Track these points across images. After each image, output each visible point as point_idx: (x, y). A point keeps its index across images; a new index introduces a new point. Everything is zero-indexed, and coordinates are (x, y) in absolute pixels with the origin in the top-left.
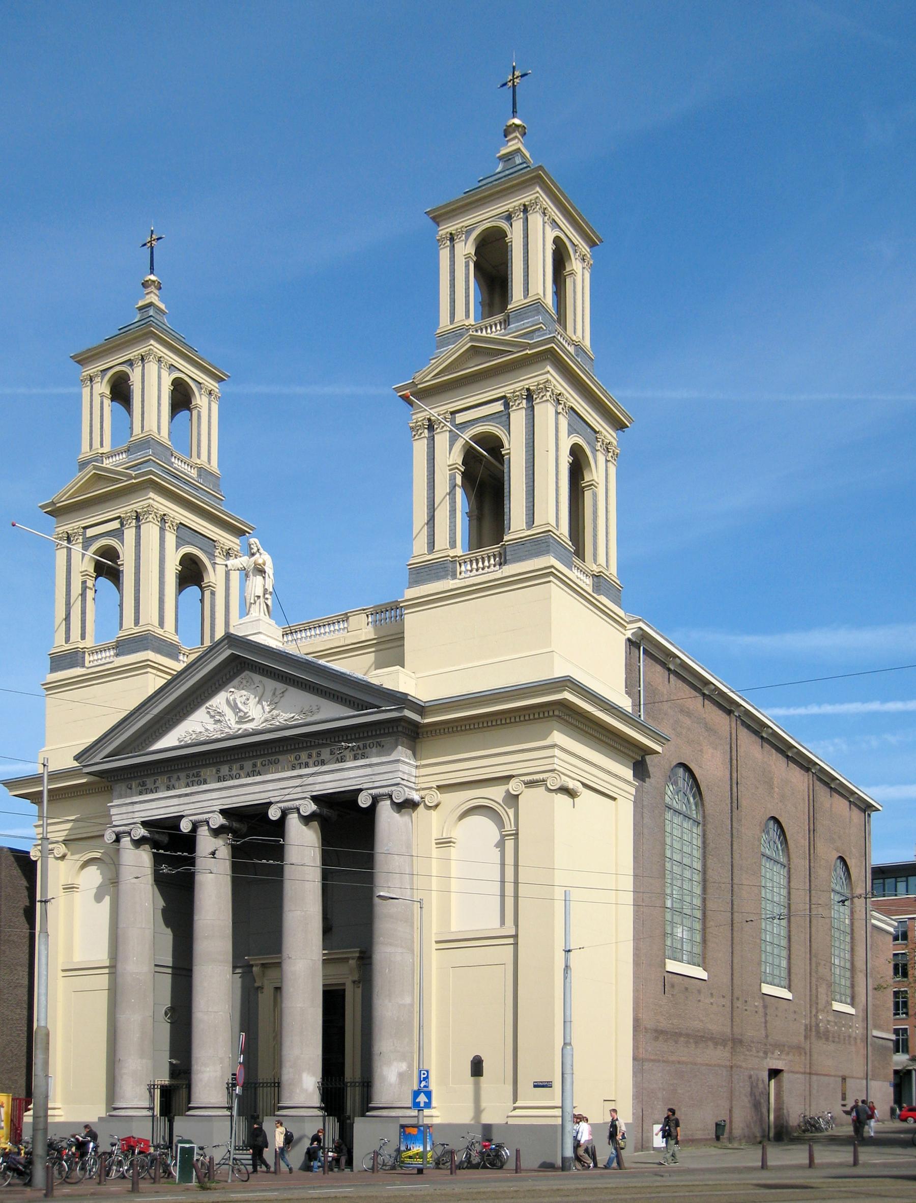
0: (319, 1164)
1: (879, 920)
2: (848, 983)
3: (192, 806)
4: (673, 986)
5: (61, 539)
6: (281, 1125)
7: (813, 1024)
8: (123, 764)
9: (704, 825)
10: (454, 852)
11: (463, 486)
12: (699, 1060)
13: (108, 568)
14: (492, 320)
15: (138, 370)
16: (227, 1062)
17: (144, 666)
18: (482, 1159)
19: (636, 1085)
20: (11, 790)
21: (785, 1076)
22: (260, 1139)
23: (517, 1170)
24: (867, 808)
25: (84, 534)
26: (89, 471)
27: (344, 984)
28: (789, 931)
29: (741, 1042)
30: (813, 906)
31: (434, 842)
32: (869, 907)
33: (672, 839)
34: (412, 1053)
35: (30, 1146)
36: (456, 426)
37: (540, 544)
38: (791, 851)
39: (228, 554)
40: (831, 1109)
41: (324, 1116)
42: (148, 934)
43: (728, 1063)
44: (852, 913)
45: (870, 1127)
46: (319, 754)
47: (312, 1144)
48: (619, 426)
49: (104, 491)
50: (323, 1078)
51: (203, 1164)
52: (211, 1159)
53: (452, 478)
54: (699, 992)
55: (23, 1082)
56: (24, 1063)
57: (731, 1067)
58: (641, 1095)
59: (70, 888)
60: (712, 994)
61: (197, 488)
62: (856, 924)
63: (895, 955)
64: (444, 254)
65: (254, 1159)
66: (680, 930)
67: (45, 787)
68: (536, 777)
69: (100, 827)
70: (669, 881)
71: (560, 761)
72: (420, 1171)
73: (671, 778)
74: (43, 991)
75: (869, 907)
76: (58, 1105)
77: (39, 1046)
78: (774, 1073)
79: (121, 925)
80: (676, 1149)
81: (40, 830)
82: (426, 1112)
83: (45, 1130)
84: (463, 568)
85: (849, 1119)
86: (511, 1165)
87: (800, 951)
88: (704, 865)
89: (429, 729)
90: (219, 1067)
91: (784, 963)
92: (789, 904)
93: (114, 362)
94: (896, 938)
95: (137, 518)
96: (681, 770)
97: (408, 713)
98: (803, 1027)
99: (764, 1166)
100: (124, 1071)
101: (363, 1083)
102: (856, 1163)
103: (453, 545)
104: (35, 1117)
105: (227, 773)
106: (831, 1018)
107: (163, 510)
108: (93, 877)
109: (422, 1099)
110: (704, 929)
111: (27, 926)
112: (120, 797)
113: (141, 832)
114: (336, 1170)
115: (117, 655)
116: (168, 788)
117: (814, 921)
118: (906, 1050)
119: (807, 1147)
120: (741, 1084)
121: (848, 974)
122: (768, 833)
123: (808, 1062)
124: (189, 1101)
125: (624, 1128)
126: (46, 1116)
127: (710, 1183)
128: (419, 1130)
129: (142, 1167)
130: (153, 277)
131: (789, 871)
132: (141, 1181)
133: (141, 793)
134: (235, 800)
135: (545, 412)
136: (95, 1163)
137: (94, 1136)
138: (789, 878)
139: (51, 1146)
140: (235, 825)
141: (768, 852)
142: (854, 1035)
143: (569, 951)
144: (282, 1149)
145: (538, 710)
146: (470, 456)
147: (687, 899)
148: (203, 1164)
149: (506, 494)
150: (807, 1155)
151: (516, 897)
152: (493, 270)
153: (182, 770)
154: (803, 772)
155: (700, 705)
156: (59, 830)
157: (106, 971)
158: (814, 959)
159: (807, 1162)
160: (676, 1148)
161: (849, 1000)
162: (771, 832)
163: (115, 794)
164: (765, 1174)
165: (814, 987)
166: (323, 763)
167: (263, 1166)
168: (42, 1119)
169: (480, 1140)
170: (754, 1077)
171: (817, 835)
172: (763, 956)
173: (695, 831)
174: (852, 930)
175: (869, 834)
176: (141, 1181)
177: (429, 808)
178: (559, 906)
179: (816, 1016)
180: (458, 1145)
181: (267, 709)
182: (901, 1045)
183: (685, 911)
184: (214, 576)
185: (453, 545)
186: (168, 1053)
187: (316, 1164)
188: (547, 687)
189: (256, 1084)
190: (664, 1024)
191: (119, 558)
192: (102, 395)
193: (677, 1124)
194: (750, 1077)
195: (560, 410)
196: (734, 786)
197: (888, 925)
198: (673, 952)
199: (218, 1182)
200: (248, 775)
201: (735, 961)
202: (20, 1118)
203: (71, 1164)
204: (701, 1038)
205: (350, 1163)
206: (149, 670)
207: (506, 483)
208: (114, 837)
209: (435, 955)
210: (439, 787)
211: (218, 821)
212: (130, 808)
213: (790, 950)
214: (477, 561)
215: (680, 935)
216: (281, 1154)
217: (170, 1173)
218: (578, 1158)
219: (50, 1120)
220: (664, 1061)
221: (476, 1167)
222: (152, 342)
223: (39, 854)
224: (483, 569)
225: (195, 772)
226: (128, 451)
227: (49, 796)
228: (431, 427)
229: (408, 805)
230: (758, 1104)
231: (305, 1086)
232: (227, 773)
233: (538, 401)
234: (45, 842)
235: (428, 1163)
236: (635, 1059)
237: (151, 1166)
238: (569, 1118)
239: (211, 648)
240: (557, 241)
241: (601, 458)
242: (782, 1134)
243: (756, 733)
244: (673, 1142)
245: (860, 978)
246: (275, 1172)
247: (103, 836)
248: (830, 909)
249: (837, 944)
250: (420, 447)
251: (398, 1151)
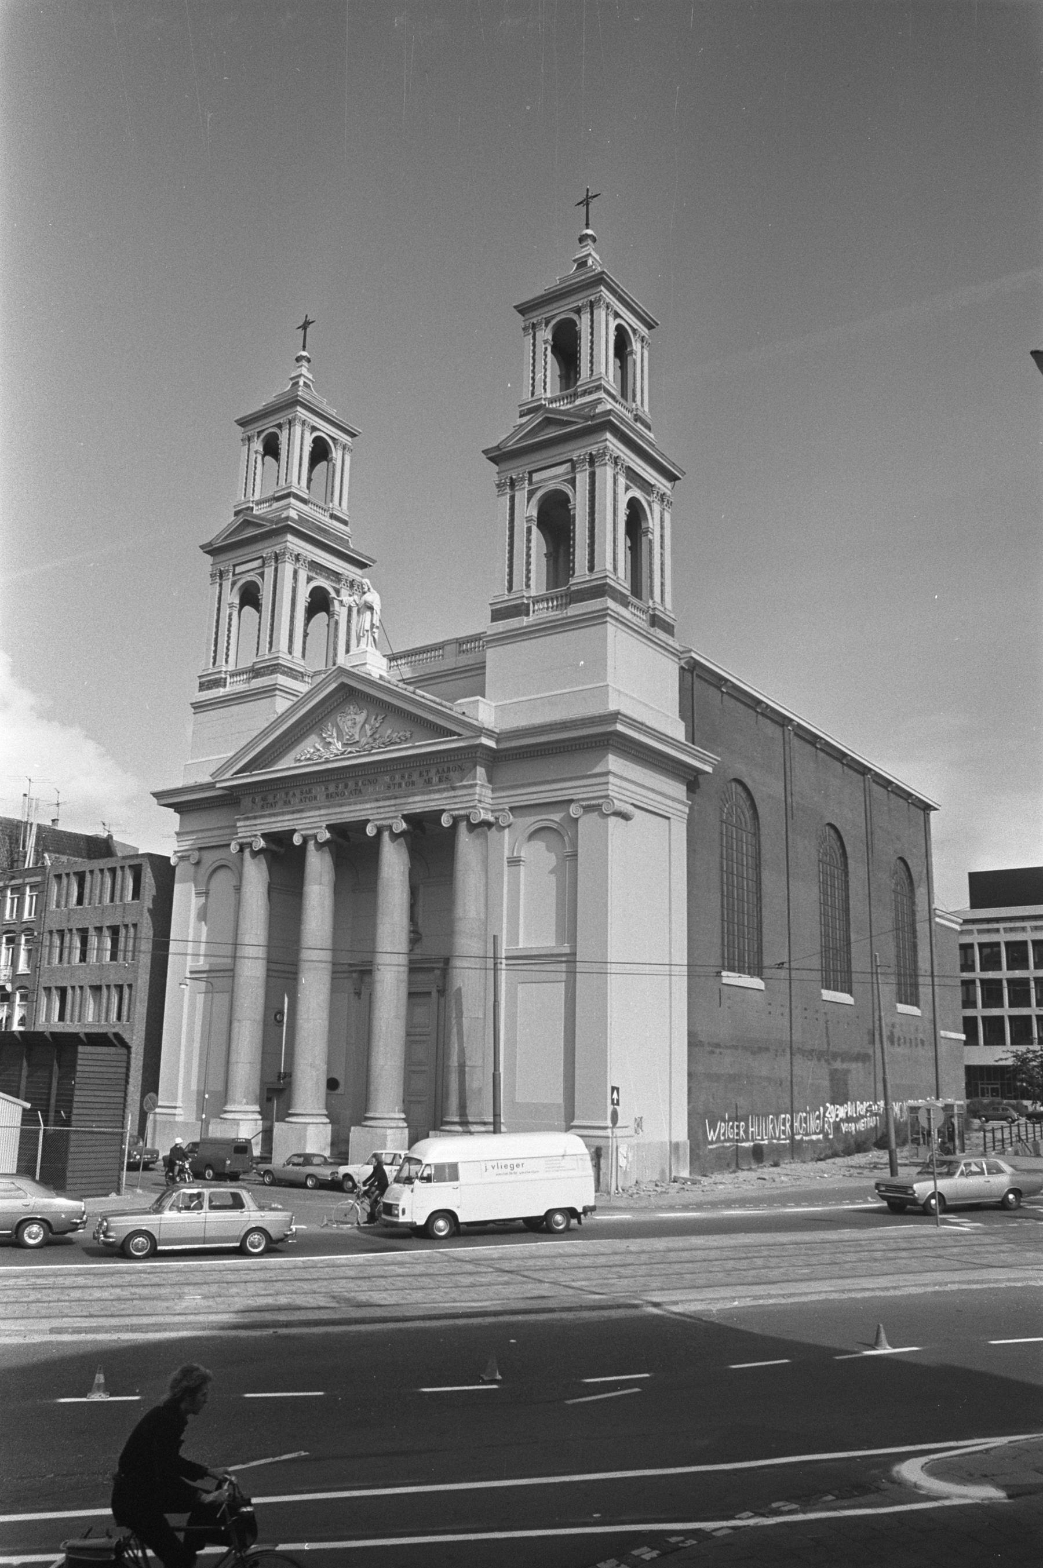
46: (410, 776)
113: (262, 843)
210: (511, 809)
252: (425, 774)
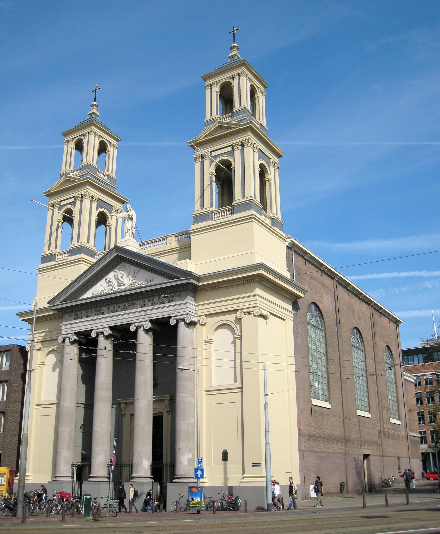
0: (150, 508)
1: (407, 376)
2: (396, 409)
3: (97, 325)
4: (315, 412)
5: (50, 206)
6: (133, 487)
7: (382, 430)
8: (69, 306)
9: (325, 332)
10: (213, 346)
11: (215, 181)
12: (330, 451)
13: (68, 218)
14: (226, 116)
15: (86, 138)
16: (108, 453)
17: (80, 260)
18: (229, 505)
19: (301, 464)
20: (20, 317)
21: (371, 458)
22: (122, 494)
23: (246, 511)
24: (396, 322)
25: (60, 204)
26: (64, 178)
27: (162, 413)
28: (367, 383)
29: (349, 440)
30: (377, 370)
31: (204, 341)
32: (403, 370)
33: (311, 339)
34: (194, 448)
35: (16, 495)
36: (212, 157)
37: (248, 205)
38: (365, 343)
39: (117, 211)
40: (393, 475)
41: (153, 482)
42: (75, 387)
43: (344, 452)
44: (395, 373)
45: (413, 483)
46: (153, 300)
47: (147, 497)
48: (279, 156)
49: (70, 186)
50: (152, 462)
51: (95, 507)
52: (99, 504)
53: (211, 178)
54: (328, 415)
55: (15, 462)
56: (16, 452)
57: (345, 454)
58: (304, 470)
59: (42, 364)
60: (334, 416)
61: (106, 184)
62: (397, 379)
63: (416, 393)
64: (208, 91)
65: (119, 505)
66: (317, 384)
67: (35, 316)
68: (249, 310)
69: (57, 335)
70: (311, 359)
71: (260, 302)
72: (199, 512)
73: (309, 309)
74: (27, 415)
75: (403, 370)
76: (30, 474)
77: (23, 443)
78: (366, 456)
79: (63, 383)
80: (322, 498)
81: (31, 336)
82: (201, 480)
83: (24, 487)
84: (216, 216)
85: (403, 479)
86: (242, 508)
87: (373, 393)
88: (326, 351)
89: (201, 288)
90: (104, 456)
91: (366, 399)
92: (366, 369)
93: (77, 135)
94: (416, 385)
95: (82, 197)
96: (313, 306)
97: (192, 281)
98: (377, 432)
99: (364, 506)
100: (61, 457)
101: (171, 464)
102: (408, 503)
103: (211, 206)
104: (19, 480)
105: (113, 309)
106: (390, 427)
107: (92, 193)
108: (52, 359)
109: (199, 473)
110: (328, 383)
111: (22, 383)
112: (66, 321)
113: (74, 337)
114: (158, 511)
115: (69, 256)
116: (87, 317)
117: (378, 378)
118: (426, 442)
119: (384, 495)
120: (351, 463)
121: (396, 404)
122: (354, 335)
123: (381, 450)
124: (90, 474)
125: (296, 488)
126: (24, 480)
127: (339, 516)
128: (198, 489)
129: (67, 508)
130: (95, 103)
131: (365, 353)
132: (66, 516)
133: (75, 319)
134: (116, 322)
135: (249, 151)
136: (45, 505)
137: (45, 491)
138: (365, 357)
139: (26, 496)
140: (115, 334)
141: (354, 344)
142: (401, 435)
143: (267, 395)
144: (133, 500)
145: (249, 279)
146: (218, 169)
147: (320, 368)
148: (95, 507)
149: (233, 184)
150: (384, 499)
151: (241, 368)
152: (227, 98)
153: (93, 308)
154: (367, 305)
155: (320, 275)
156: (39, 337)
157: (55, 405)
158: (380, 397)
159: (385, 503)
160: (322, 498)
161: (397, 417)
162: (355, 334)
163: (64, 319)
164: (365, 510)
165: (381, 411)
166: (155, 304)
167: (124, 509)
168: (22, 481)
169: (227, 495)
170: (356, 459)
171: (376, 335)
172: (356, 396)
173: (321, 334)
174: (396, 382)
175: (399, 334)
176: (66, 516)
177: (201, 325)
178: (261, 372)
179: (383, 426)
180: (217, 497)
181: (131, 279)
182: (423, 440)
183: (319, 374)
184: (111, 221)
185: (211, 206)
186: (81, 448)
187: (149, 508)
188: (252, 268)
189: (121, 465)
190: (313, 432)
191: (73, 214)
192: (72, 148)
193: (322, 485)
194: (355, 459)
195: (255, 150)
196: (337, 312)
197: (412, 378)
198: (315, 394)
199: (102, 517)
200: (122, 310)
201: (344, 399)
202: (13, 480)
203: (34, 505)
204: (330, 439)
205: (165, 507)
206: (82, 262)
207: (233, 180)
208: (62, 340)
209: (205, 398)
210: (206, 315)
211: (108, 332)
212: (70, 326)
213: (368, 392)
214: (221, 212)
215: (317, 386)
216: (132, 502)
217: (80, 512)
218: (275, 504)
219: (26, 482)
220: (313, 452)
221: (225, 509)
222: (93, 127)
223: (29, 348)
224: (224, 216)
225: (99, 309)
226: (80, 170)
227: (36, 320)
228: (202, 157)
229: (192, 324)
230: (359, 473)
231: (144, 466)
232: (113, 309)
234: (33, 342)
235: (202, 507)
237: (71, 508)
238: (269, 482)
239: (109, 252)
240: (251, 86)
241: (272, 169)
242: (371, 489)
243: (345, 288)
244: (320, 494)
245: (402, 406)
246: (129, 512)
247: (57, 339)
248: (385, 371)
249: (390, 389)
250: (198, 166)
251: (188, 501)
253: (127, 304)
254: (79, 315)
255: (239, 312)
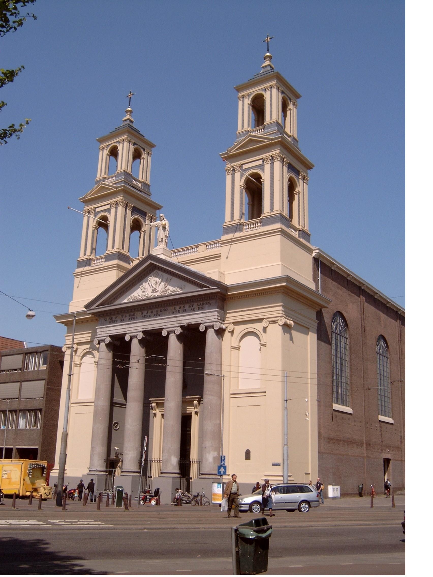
20: (57, 320)
46: (184, 307)
64: (240, 103)
84: (245, 227)
105: (146, 314)
146: (248, 182)
204: (350, 442)
208: (97, 342)
212: (105, 329)
220: (333, 454)
232: (146, 314)
233: (276, 160)
236: (319, 452)
240: (283, 98)
252: (191, 306)
253: (159, 309)
254: (114, 319)
255: (264, 321)
